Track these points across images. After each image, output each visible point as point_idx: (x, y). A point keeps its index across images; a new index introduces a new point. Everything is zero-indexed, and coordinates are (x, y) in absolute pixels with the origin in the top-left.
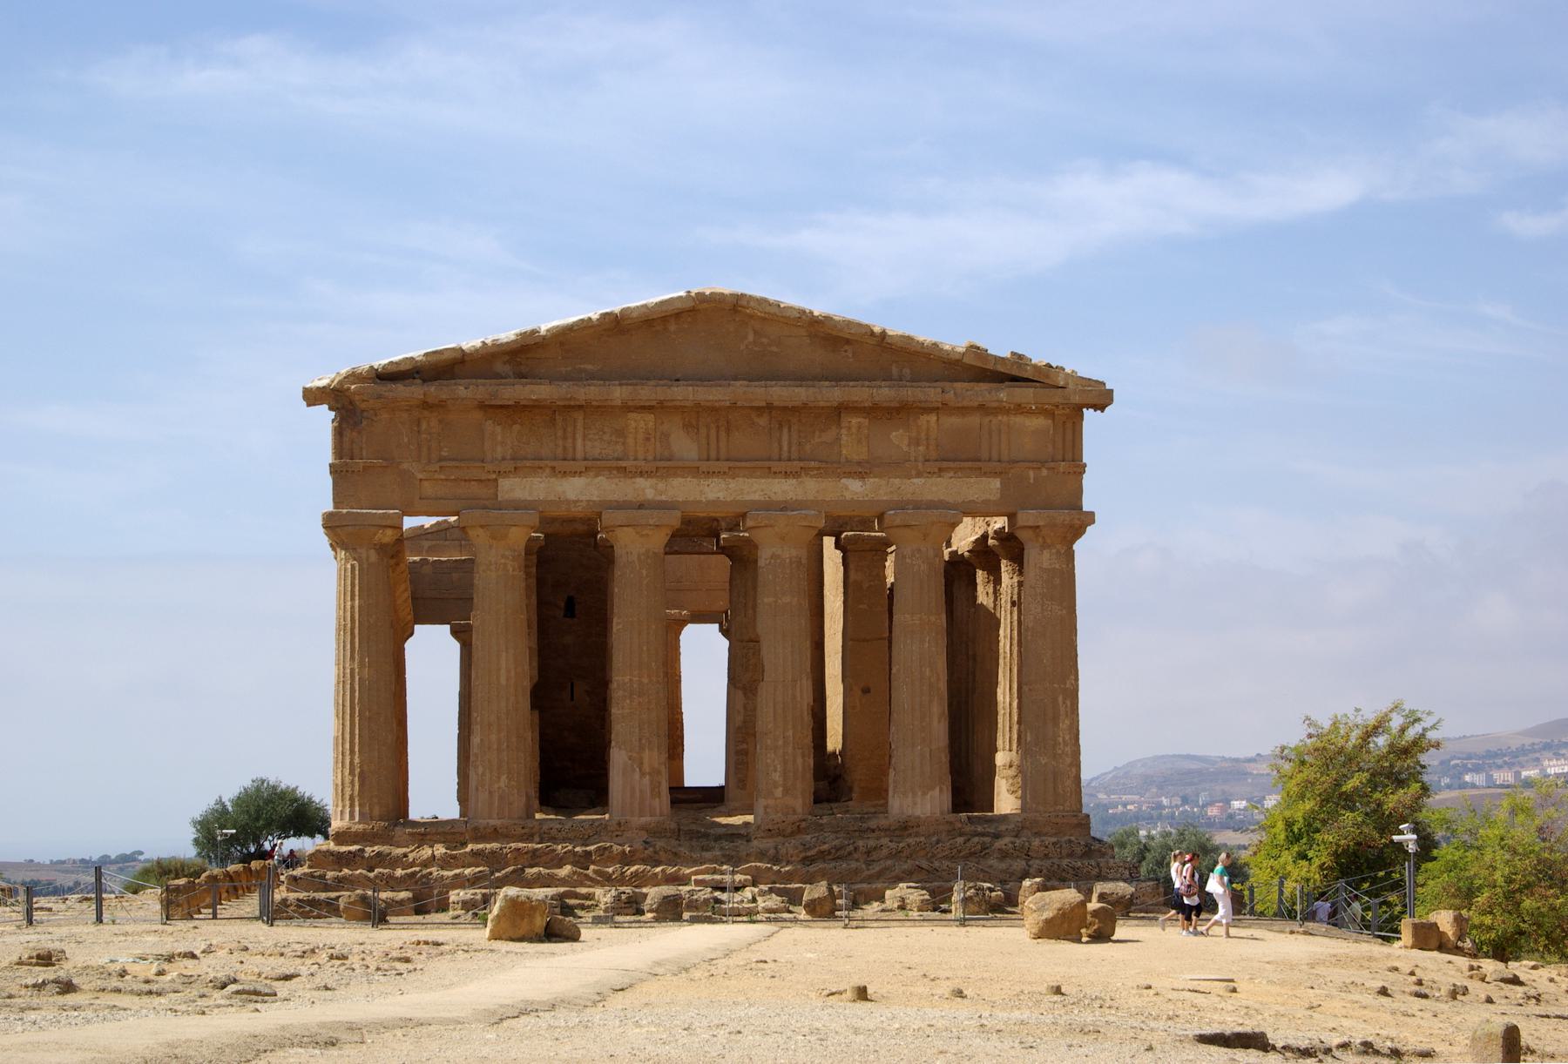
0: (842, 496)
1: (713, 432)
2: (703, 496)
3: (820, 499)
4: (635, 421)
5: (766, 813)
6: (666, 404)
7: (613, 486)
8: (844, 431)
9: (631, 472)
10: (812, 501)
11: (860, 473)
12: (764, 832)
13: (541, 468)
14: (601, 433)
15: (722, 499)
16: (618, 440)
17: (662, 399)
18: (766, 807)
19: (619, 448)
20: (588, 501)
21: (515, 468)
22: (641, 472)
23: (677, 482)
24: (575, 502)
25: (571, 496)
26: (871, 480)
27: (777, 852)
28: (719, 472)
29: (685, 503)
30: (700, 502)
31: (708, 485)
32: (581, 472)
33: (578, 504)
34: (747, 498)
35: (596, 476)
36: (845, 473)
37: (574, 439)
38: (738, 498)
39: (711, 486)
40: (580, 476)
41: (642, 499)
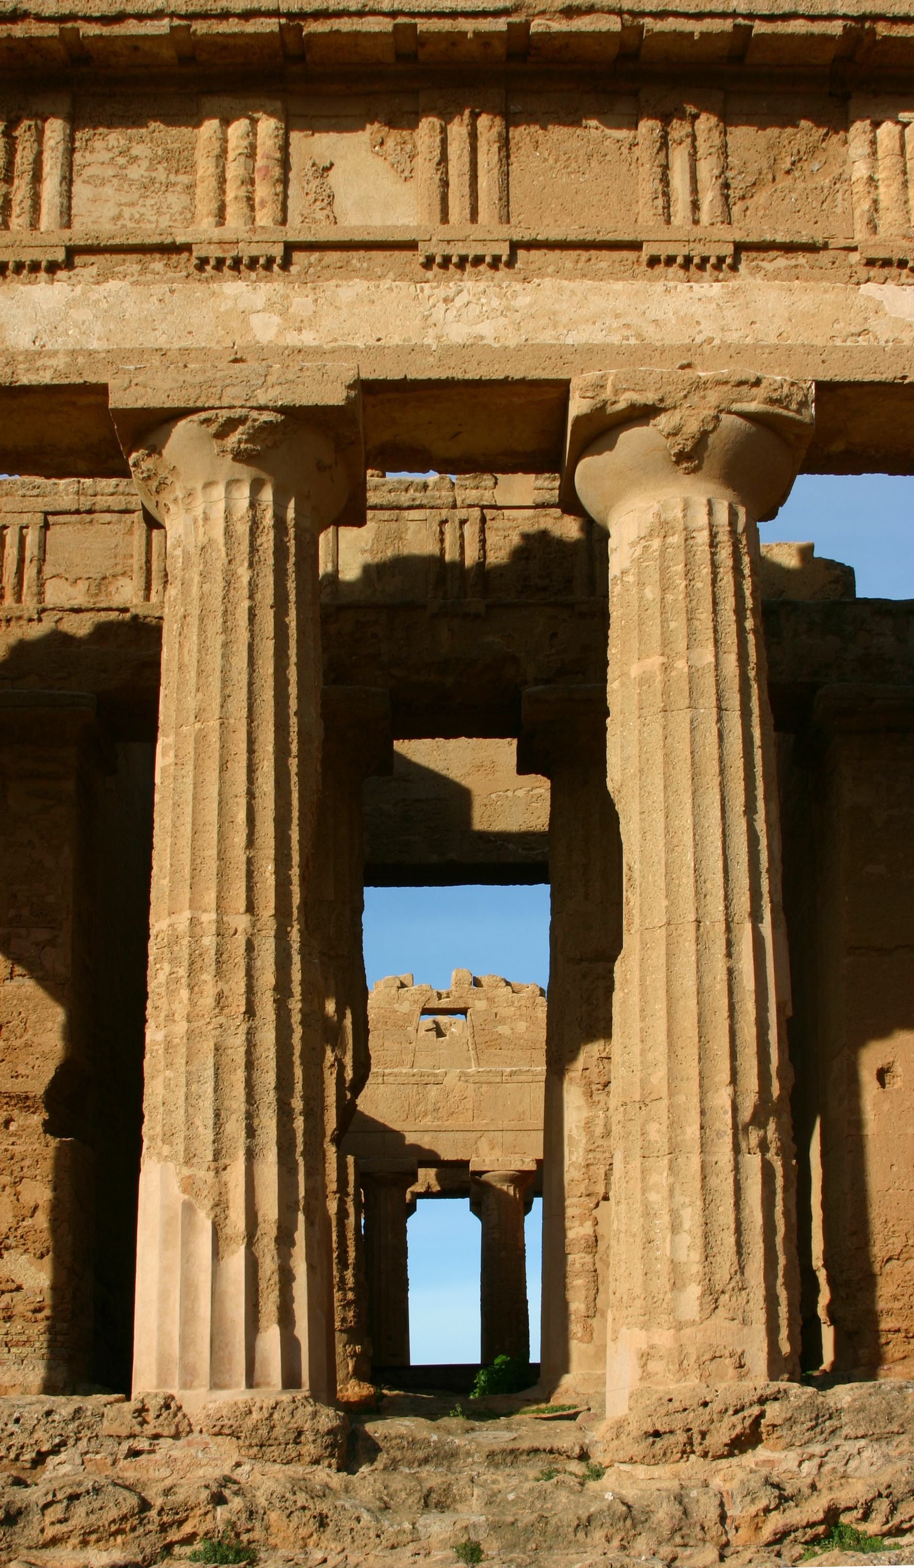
2: (431, 332)
5: (645, 1376)
7: (153, 305)
9: (203, 263)
12: (637, 1441)
14: (121, 161)
15: (489, 341)
16: (172, 178)
18: (645, 1357)
19: (176, 200)
20: (73, 353)
24: (32, 356)
27: (685, 1512)
29: (377, 351)
30: (425, 350)
32: (53, 268)
33: (39, 363)
35: (102, 278)
37: (37, 178)
38: (547, 337)
39: (459, 301)
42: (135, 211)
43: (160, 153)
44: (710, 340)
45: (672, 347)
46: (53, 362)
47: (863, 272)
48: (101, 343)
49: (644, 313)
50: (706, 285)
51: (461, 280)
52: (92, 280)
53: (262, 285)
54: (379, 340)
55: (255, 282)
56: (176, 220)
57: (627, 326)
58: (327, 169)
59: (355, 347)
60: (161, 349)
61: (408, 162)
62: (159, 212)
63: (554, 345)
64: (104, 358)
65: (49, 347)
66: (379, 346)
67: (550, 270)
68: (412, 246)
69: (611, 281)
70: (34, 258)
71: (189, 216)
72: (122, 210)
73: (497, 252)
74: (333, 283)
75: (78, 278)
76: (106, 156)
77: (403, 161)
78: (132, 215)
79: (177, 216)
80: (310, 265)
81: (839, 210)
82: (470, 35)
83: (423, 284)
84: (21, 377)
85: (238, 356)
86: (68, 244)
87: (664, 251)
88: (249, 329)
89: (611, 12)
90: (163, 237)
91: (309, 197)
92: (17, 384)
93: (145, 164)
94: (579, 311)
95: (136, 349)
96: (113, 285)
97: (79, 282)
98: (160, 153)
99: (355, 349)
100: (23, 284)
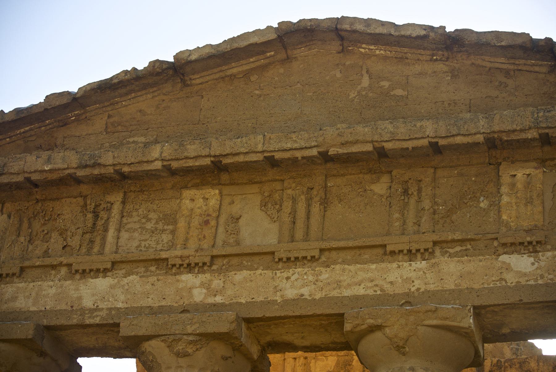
0: (501, 279)
1: (301, 207)
3: (464, 286)
4: (192, 200)
6: (227, 161)
7: (149, 287)
8: (504, 189)
9: (174, 265)
10: (453, 290)
11: (530, 243)
13: (53, 267)
14: (144, 220)
16: (166, 227)
17: (217, 153)
19: (166, 238)
20: (110, 309)
21: (22, 269)
22: (189, 265)
23: (240, 276)
24: (92, 311)
25: (88, 303)
26: (549, 254)
28: (305, 258)
29: (251, 304)
31: (288, 278)
32: (106, 271)
34: (347, 293)
36: (504, 245)
38: (335, 293)
39: (293, 278)
40: (105, 277)
41: (187, 302)
42: (146, 243)
43: (161, 216)
44: (418, 289)
45: (399, 294)
46: (101, 313)
47: (501, 250)
48: (123, 304)
49: (385, 278)
50: (419, 263)
51: (295, 268)
52: (122, 276)
53: (200, 275)
54: (253, 298)
55: (197, 274)
56: (165, 247)
57: (376, 285)
58: (238, 219)
59: (240, 302)
60: (150, 307)
61: (276, 214)
62: (158, 243)
63: (339, 297)
64: (124, 311)
65: (100, 307)
66: (252, 302)
67: (340, 260)
68: (273, 253)
69: (370, 264)
70: (98, 267)
71: (171, 244)
72: (141, 243)
73: (313, 254)
74: (233, 273)
75: (117, 275)
76: (136, 219)
77: (274, 213)
78: (145, 245)
79: (165, 245)
80: (223, 265)
81: (491, 220)
82: (300, 158)
83: (277, 271)
84: (86, 320)
85: (186, 309)
86: (113, 261)
87: (397, 248)
88: (192, 296)
89: (367, 142)
90: (156, 256)
91: (228, 233)
92: (85, 323)
93: (154, 222)
94: (353, 280)
95: (139, 307)
96: (131, 278)
97: (117, 277)
98: (161, 216)
99: (241, 303)
100: (92, 278)
